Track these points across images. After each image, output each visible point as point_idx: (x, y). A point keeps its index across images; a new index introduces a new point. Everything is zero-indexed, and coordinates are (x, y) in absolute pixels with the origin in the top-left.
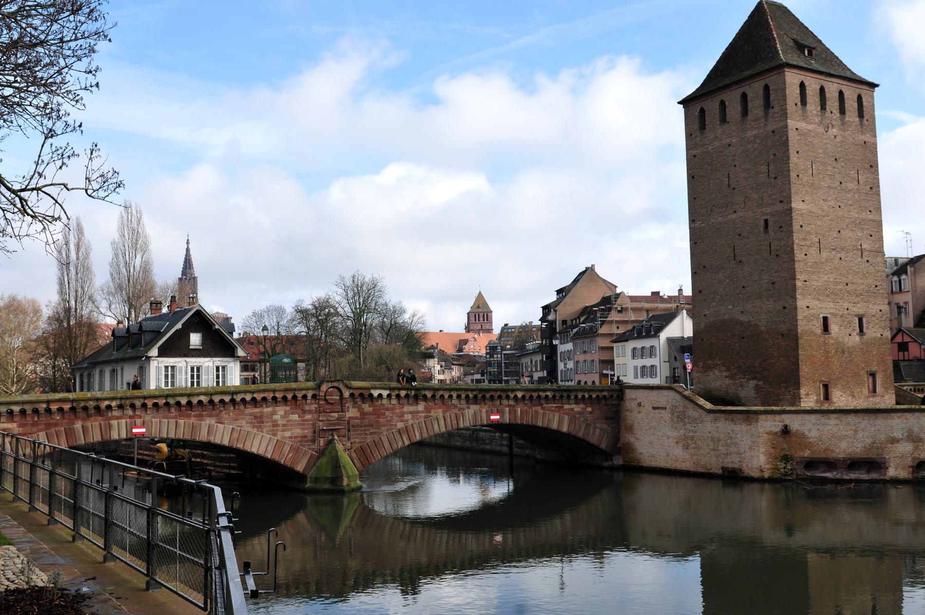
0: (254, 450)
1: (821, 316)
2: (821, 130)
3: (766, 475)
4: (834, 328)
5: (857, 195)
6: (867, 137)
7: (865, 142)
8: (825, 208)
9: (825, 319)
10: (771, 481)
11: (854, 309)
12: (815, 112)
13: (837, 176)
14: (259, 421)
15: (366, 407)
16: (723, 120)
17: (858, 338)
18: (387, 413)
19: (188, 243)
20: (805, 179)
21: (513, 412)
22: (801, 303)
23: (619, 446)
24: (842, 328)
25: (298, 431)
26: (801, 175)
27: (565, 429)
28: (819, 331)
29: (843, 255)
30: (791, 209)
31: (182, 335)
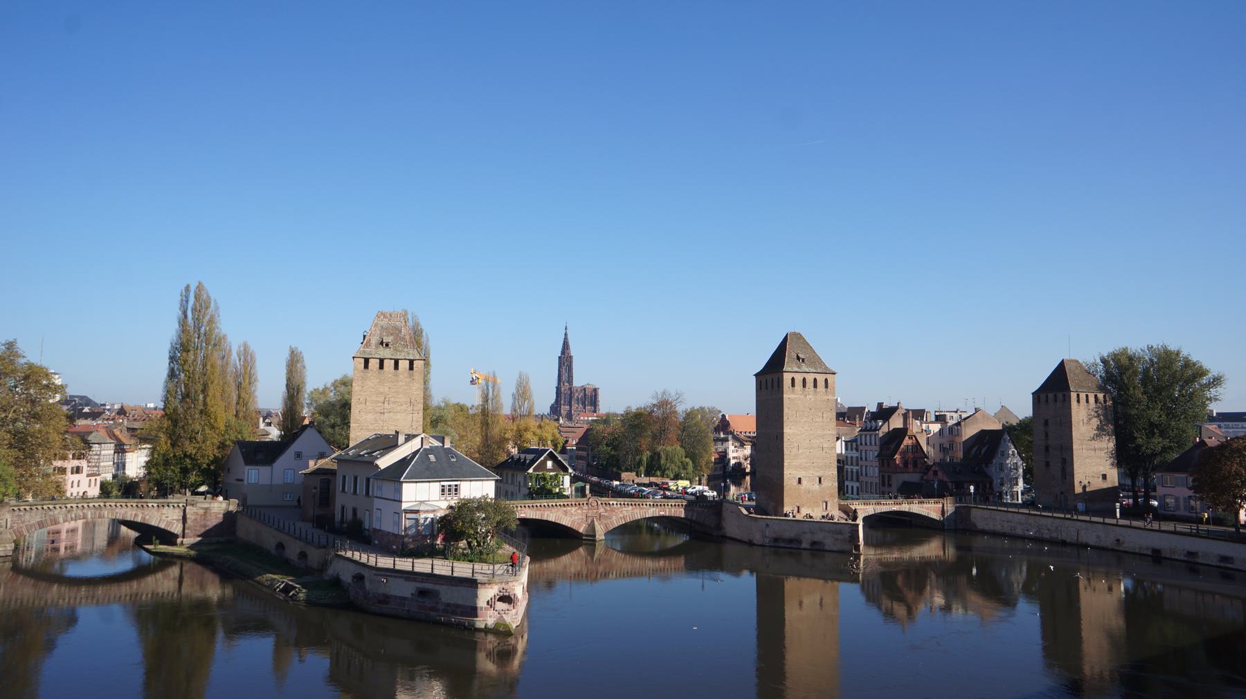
0: (564, 524)
3: (760, 543)
4: (804, 482)
5: (821, 424)
6: (830, 397)
9: (800, 479)
10: (761, 545)
14: (566, 512)
15: (608, 508)
16: (767, 388)
17: (818, 486)
18: (616, 511)
19: (566, 329)
20: (792, 419)
21: (670, 511)
22: (786, 472)
23: (719, 527)
25: (581, 517)
27: (694, 518)
30: (783, 433)
31: (544, 462)
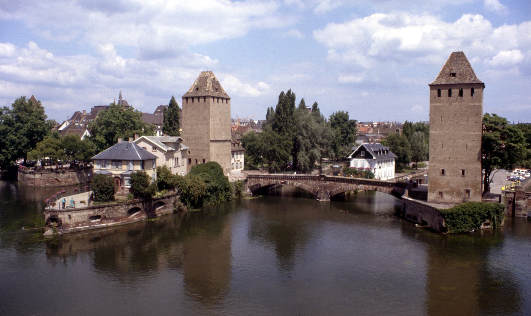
1: (441, 169)
2: (448, 104)
4: (447, 173)
5: (466, 127)
6: (476, 104)
7: (474, 106)
8: (447, 132)
11: (459, 167)
12: (445, 99)
13: (454, 120)
14: (306, 183)
20: (437, 123)
24: (452, 174)
26: (435, 122)
28: (440, 174)
29: (455, 148)
